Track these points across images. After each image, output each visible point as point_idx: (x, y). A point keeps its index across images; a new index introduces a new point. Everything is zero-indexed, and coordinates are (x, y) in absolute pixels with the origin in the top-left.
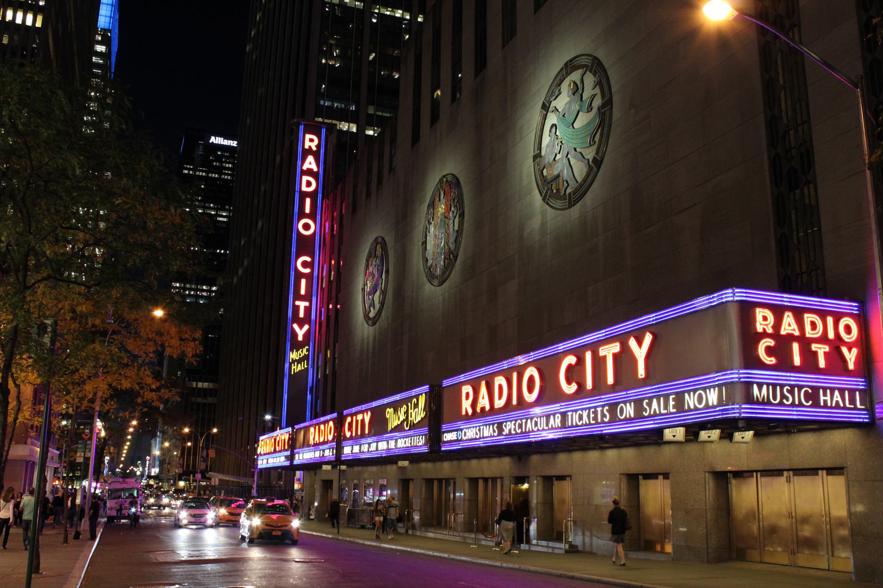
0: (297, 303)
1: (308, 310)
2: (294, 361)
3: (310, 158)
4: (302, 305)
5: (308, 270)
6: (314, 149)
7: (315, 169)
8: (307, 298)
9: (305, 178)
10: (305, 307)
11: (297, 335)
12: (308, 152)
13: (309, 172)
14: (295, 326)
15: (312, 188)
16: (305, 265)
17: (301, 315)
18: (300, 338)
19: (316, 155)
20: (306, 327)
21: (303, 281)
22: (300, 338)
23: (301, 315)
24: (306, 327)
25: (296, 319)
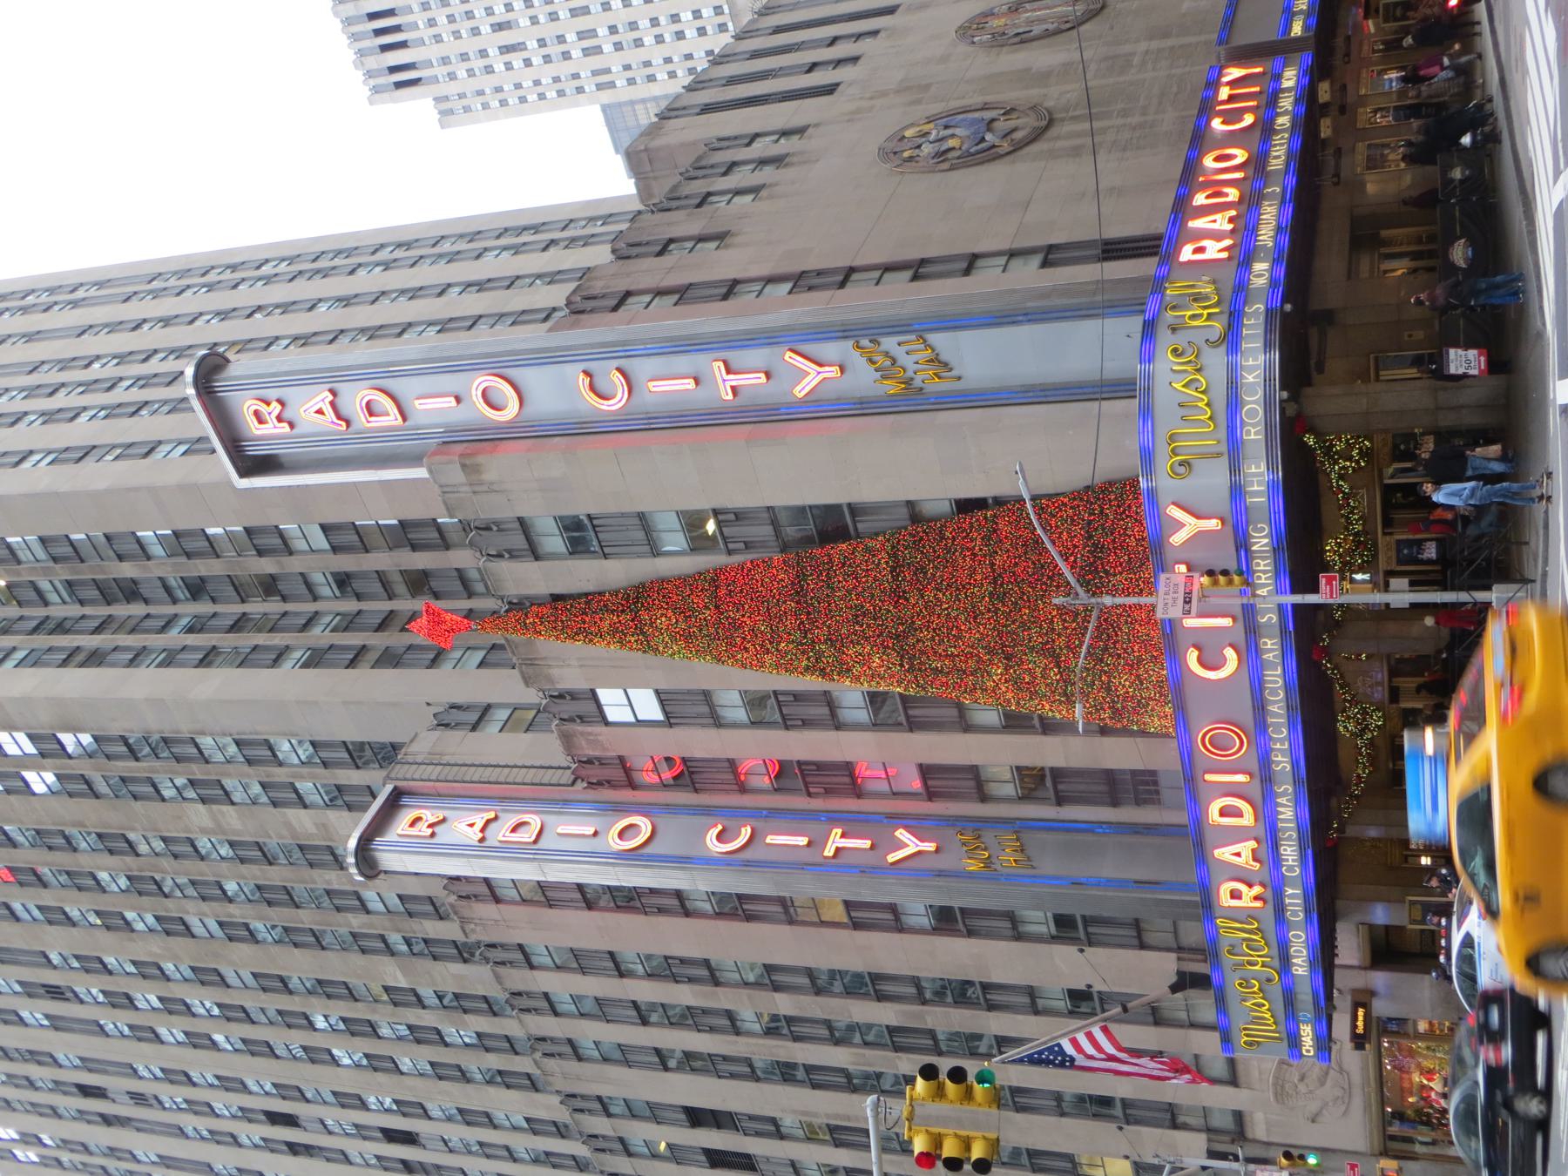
5: (746, 832)
7: (492, 815)
10: (843, 836)
11: (920, 852)
18: (930, 847)
22: (930, 847)
24: (901, 834)
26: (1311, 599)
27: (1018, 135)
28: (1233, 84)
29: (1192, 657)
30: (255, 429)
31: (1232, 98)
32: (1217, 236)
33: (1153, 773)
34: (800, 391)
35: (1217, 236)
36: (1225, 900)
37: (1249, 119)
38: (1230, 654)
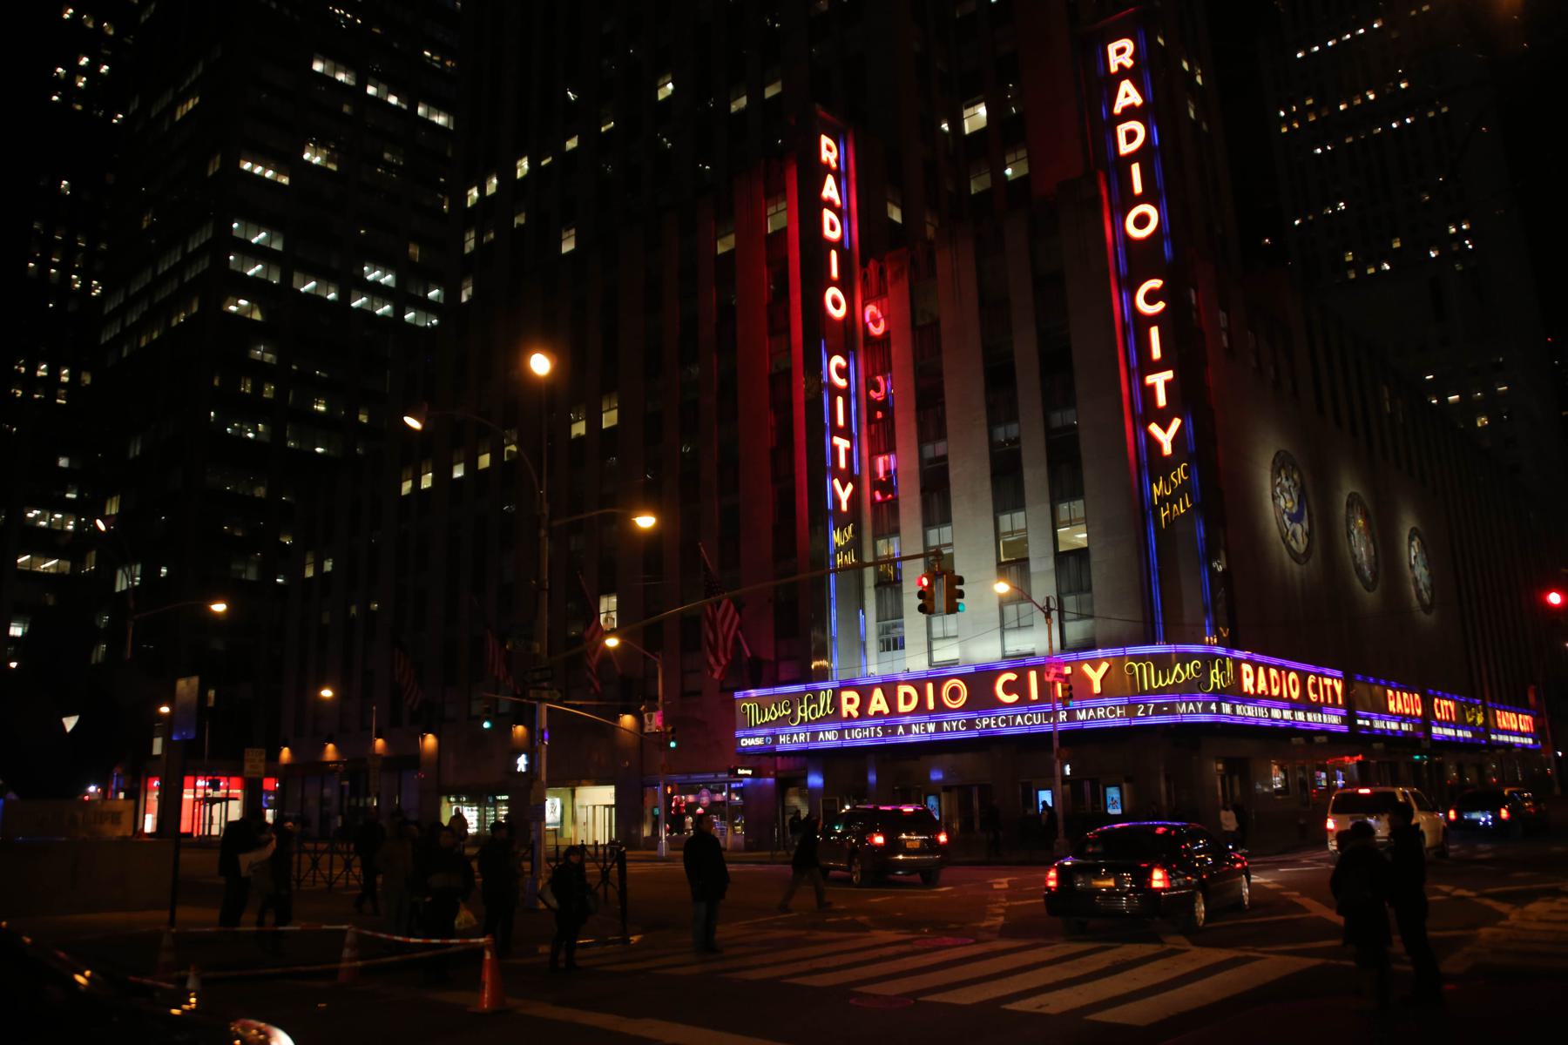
0: (837, 440)
1: (849, 453)
2: (839, 549)
3: (830, 181)
4: (842, 444)
5: (842, 383)
6: (834, 165)
7: (838, 202)
8: (845, 433)
9: (828, 215)
12: (826, 169)
13: (830, 204)
14: (836, 482)
15: (835, 235)
16: (842, 372)
17: (842, 464)
18: (844, 507)
19: (838, 176)
20: (850, 487)
21: (840, 400)
22: (844, 507)
23: (842, 464)
24: (850, 487)
25: (836, 472)
26: (1056, 744)
27: (1293, 544)
28: (1333, 687)
29: (1012, 677)
30: (1112, 48)
31: (1325, 687)
32: (1255, 685)
33: (903, 647)
34: (1154, 428)
35: (1255, 685)
36: (845, 695)
37: (1312, 696)
38: (1014, 698)
